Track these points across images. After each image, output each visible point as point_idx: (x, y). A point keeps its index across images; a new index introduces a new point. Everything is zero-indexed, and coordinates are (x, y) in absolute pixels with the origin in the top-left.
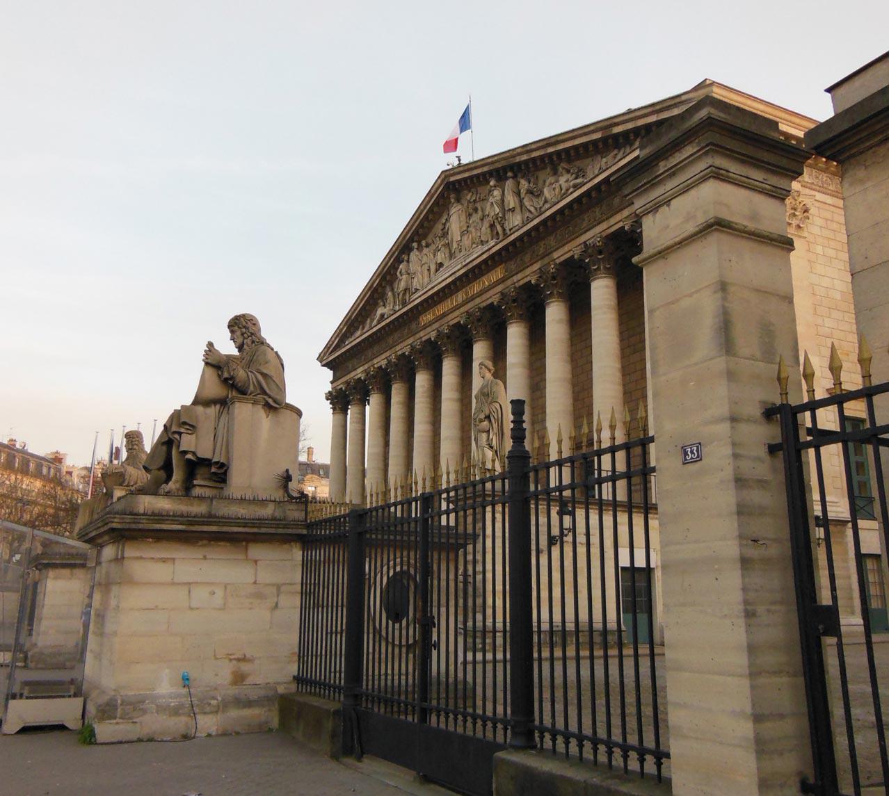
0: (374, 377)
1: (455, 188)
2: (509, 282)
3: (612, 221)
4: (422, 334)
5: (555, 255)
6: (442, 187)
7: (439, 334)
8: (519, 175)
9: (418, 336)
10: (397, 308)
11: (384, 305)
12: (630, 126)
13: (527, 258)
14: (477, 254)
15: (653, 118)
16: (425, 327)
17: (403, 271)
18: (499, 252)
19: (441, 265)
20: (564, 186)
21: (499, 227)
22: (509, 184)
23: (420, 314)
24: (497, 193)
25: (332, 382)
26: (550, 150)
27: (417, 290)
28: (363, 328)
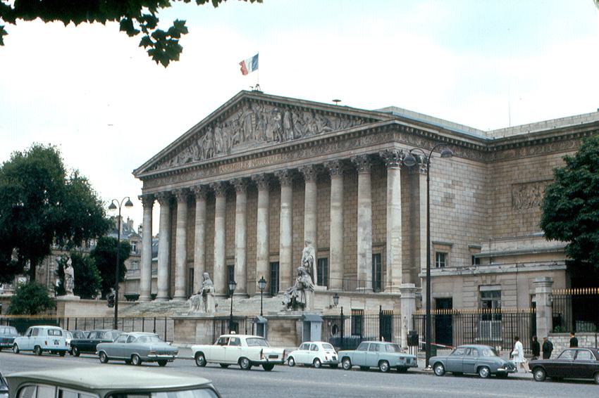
1: (248, 100)
6: (241, 98)
8: (293, 110)
14: (263, 146)
18: (279, 150)
19: (238, 142)
20: (319, 126)
24: (279, 117)
25: (142, 189)
26: (313, 107)
27: (219, 152)
28: (172, 161)
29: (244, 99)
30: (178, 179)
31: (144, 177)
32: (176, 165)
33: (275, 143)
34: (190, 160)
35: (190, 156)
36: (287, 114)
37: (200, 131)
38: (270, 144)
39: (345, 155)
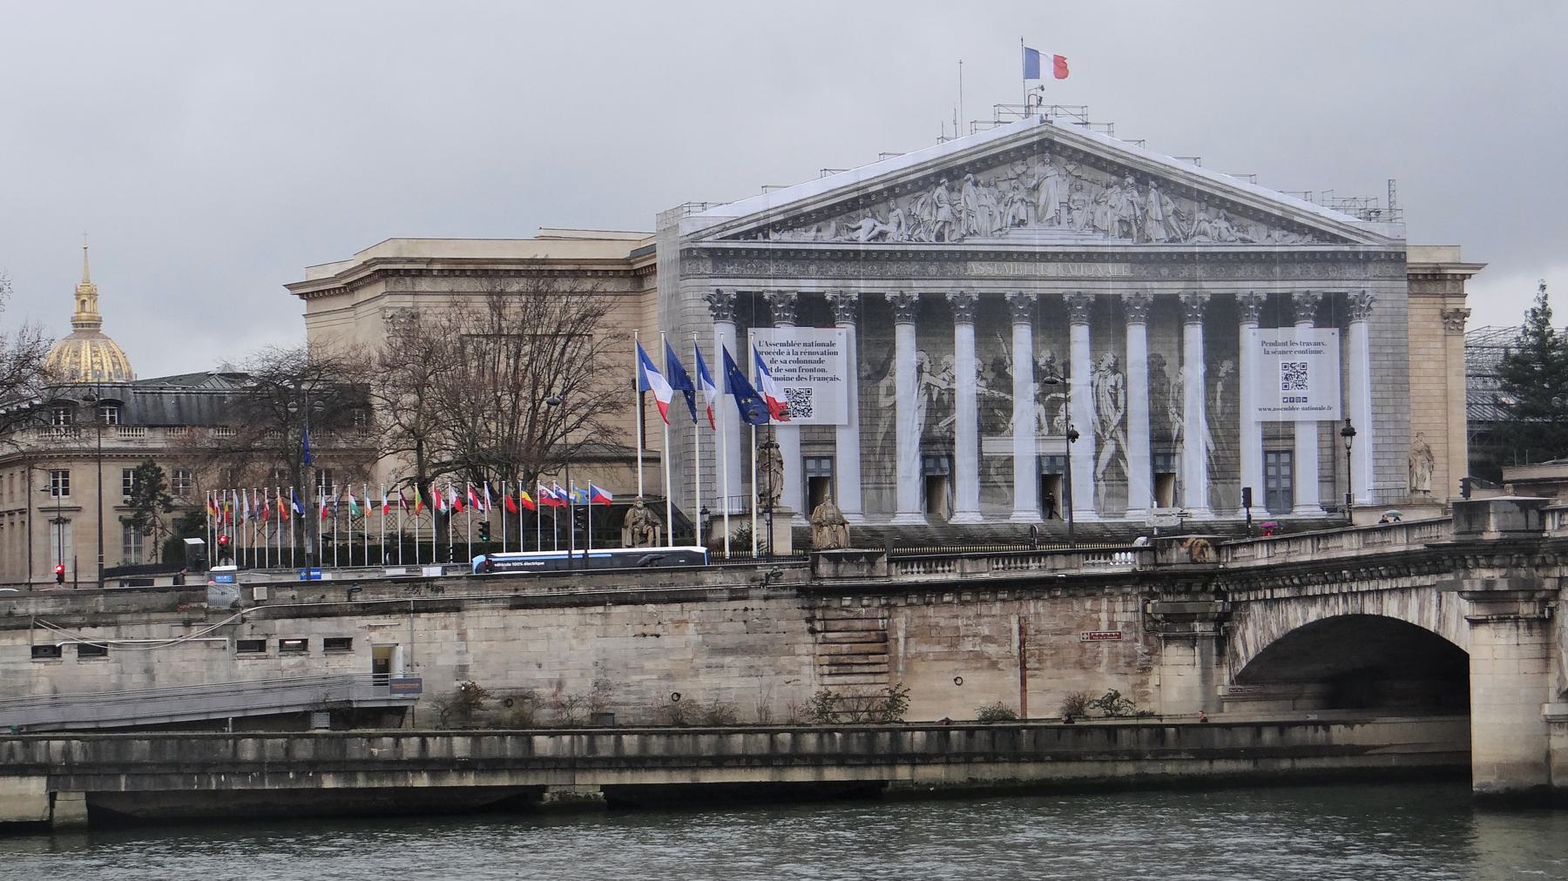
0: (852, 303)
1: (1046, 147)
2: (1139, 285)
3: (1274, 284)
4: (974, 283)
5: (1205, 285)
7: (1021, 298)
9: (964, 283)
10: (923, 236)
11: (874, 216)
12: (1312, 224)
13: (1165, 271)
15: (1335, 231)
16: (980, 278)
17: (944, 198)
19: (1022, 222)
21: (1135, 229)
22: (1153, 195)
23: (972, 260)
24: (1135, 193)
26: (1218, 193)
28: (819, 230)
29: (1040, 142)
30: (835, 270)
31: (728, 249)
32: (826, 238)
33: (1128, 242)
34: (882, 234)
35: (880, 227)
36: (1153, 195)
37: (914, 182)
38: (1118, 242)
39: (1279, 287)
